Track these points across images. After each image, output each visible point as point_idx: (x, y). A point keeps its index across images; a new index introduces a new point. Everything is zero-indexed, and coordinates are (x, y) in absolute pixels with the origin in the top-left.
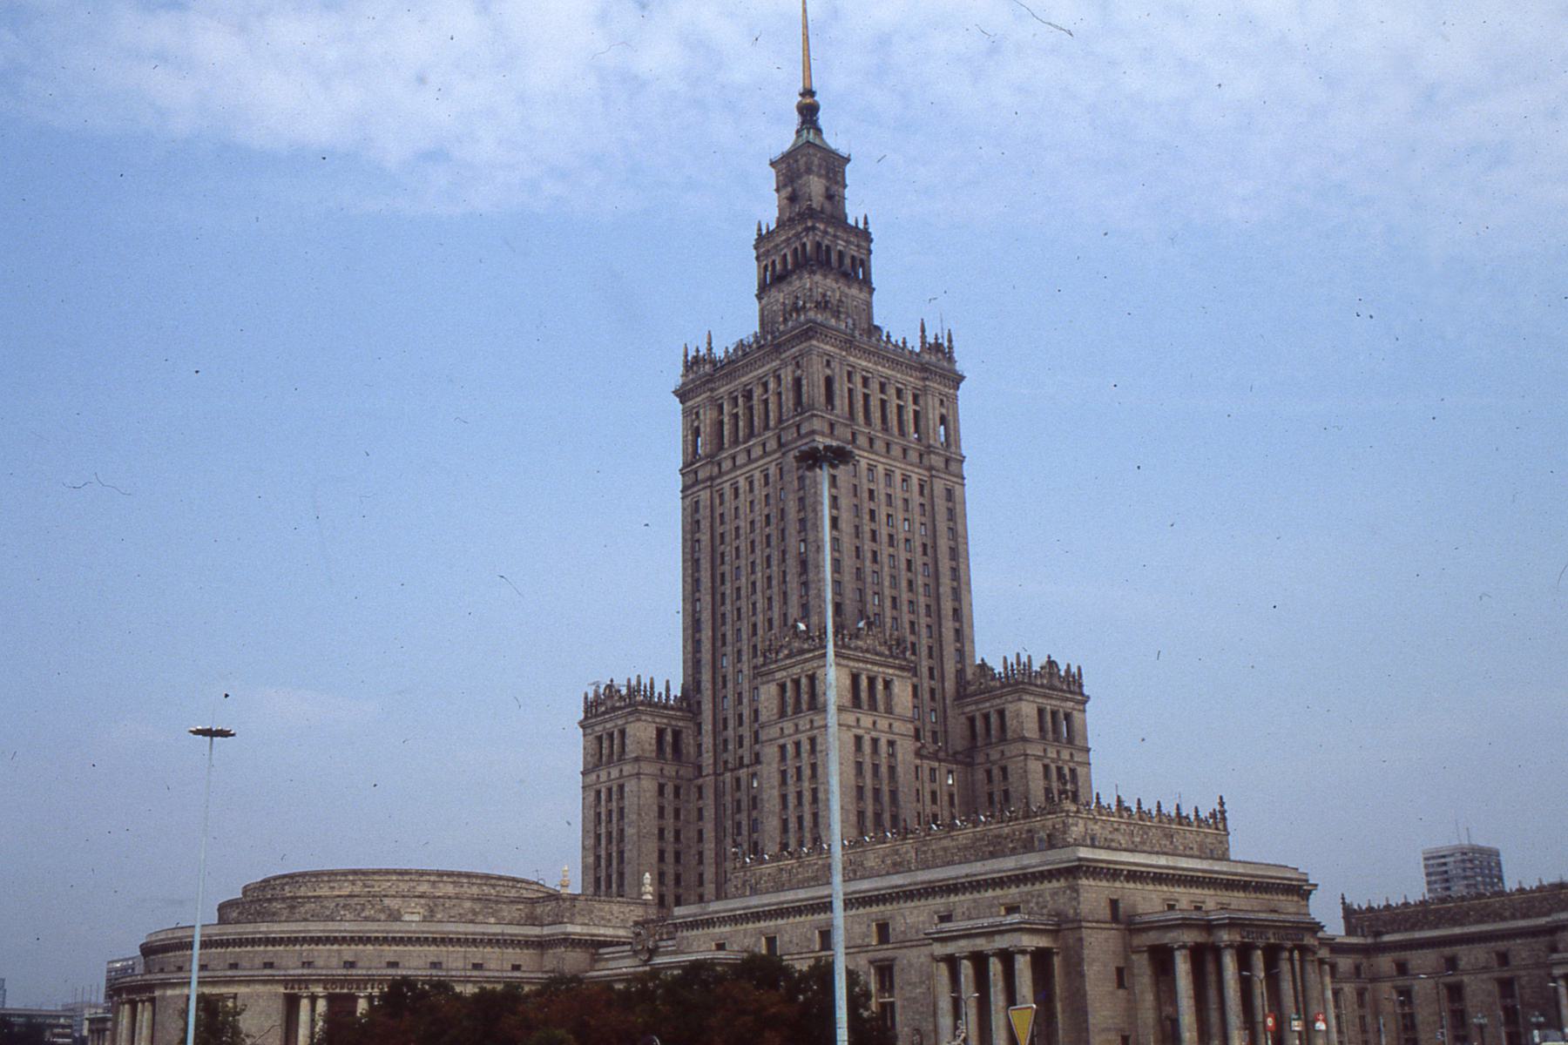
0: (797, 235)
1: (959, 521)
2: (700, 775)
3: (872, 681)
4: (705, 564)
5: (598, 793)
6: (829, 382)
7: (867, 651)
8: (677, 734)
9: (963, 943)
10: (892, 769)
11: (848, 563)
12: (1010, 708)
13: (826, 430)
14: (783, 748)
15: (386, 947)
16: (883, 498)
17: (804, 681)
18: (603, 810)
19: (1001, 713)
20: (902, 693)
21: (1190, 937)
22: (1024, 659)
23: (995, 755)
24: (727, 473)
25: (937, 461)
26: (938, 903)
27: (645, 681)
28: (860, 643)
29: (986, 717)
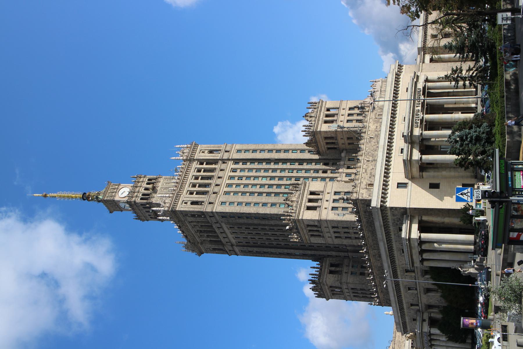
2: (348, 257)
3: (310, 201)
4: (265, 250)
5: (354, 296)
6: (193, 203)
7: (298, 202)
9: (414, 257)
12: (323, 135)
14: (336, 237)
18: (361, 295)
19: (326, 138)
20: (316, 186)
23: (343, 141)
24: (230, 240)
26: (396, 253)
27: (310, 277)
28: (294, 205)
29: (327, 143)
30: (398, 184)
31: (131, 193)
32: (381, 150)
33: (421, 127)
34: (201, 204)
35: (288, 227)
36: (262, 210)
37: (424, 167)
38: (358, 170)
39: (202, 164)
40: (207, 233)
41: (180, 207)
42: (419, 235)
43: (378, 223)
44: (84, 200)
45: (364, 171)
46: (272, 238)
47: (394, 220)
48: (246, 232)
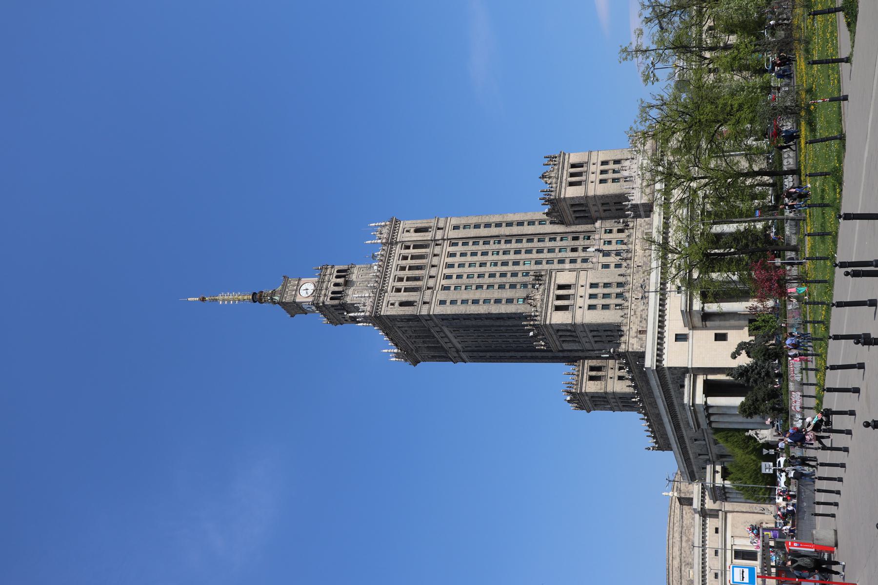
3: (559, 298)
6: (402, 304)
7: (542, 300)
8: (592, 369)
9: (700, 420)
10: (606, 285)
11: (496, 294)
12: (569, 202)
13: (427, 306)
17: (560, 334)
19: (572, 205)
20: (564, 278)
21: (697, 305)
23: (596, 208)
28: (539, 305)
29: (575, 211)
31: (318, 290)
35: (531, 334)
36: (495, 309)
37: (706, 317)
38: (626, 311)
39: (408, 247)
40: (423, 338)
41: (386, 311)
43: (654, 382)
44: (255, 302)
45: (632, 313)
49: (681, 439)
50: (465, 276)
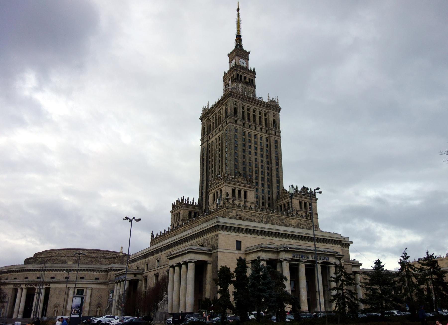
0: (233, 73)
1: (279, 149)
3: (240, 192)
4: (205, 165)
6: (236, 109)
7: (239, 182)
13: (234, 122)
15: (51, 272)
16: (253, 142)
20: (251, 196)
22: (295, 186)
25: (272, 132)
27: (186, 198)
28: (236, 180)
29: (285, 205)
30: (241, 242)
32: (272, 227)
33: (292, 260)
34: (235, 115)
38: (254, 209)
39: (265, 115)
42: (193, 261)
44: (236, 36)
45: (253, 214)
46: (213, 169)
47: (208, 239)
48: (217, 149)
49: (160, 250)
50: (250, 144)
